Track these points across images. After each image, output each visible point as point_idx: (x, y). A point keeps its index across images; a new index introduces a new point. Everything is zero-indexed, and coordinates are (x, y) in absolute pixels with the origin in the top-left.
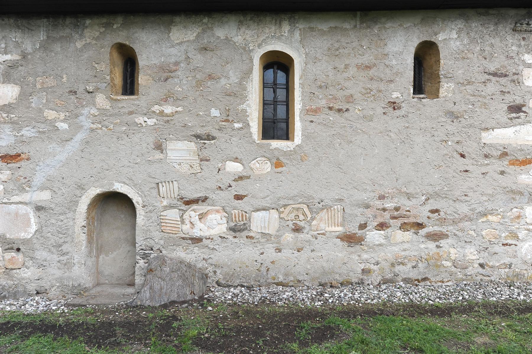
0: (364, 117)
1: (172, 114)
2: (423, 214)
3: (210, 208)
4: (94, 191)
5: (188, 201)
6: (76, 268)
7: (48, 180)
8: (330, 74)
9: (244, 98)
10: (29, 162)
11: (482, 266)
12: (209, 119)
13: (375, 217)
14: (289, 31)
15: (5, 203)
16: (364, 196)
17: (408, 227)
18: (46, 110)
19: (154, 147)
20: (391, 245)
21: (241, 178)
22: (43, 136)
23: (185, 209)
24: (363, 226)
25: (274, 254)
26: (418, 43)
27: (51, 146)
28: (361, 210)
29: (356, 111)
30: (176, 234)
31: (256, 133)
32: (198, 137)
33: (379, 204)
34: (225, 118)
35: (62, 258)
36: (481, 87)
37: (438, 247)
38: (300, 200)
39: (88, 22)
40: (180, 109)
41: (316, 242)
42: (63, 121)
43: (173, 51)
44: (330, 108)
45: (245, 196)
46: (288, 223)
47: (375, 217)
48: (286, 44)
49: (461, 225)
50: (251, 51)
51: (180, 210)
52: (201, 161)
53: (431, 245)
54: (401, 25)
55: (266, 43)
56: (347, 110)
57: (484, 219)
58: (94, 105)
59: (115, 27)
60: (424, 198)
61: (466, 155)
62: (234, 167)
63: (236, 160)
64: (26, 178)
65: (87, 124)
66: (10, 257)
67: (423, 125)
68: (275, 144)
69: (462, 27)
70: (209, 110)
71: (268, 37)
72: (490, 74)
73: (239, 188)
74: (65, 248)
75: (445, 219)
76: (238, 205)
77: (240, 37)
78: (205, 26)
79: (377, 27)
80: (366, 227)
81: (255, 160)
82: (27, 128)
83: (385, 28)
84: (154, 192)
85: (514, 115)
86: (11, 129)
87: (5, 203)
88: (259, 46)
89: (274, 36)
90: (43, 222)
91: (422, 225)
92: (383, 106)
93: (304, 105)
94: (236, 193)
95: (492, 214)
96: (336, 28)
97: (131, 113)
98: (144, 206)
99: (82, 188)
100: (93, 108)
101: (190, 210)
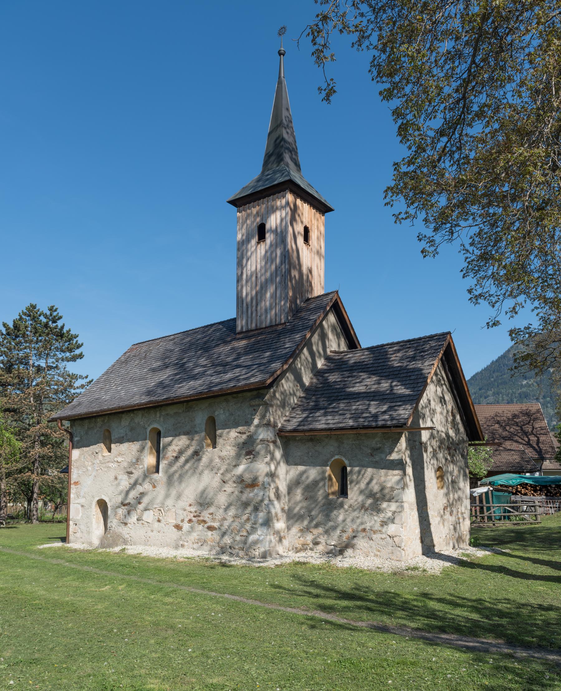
13: (187, 515)
24: (182, 521)
28: (182, 511)
43: (122, 431)
54: (200, 408)
85: (248, 457)
88: (149, 426)
97: (108, 462)
99: (93, 497)
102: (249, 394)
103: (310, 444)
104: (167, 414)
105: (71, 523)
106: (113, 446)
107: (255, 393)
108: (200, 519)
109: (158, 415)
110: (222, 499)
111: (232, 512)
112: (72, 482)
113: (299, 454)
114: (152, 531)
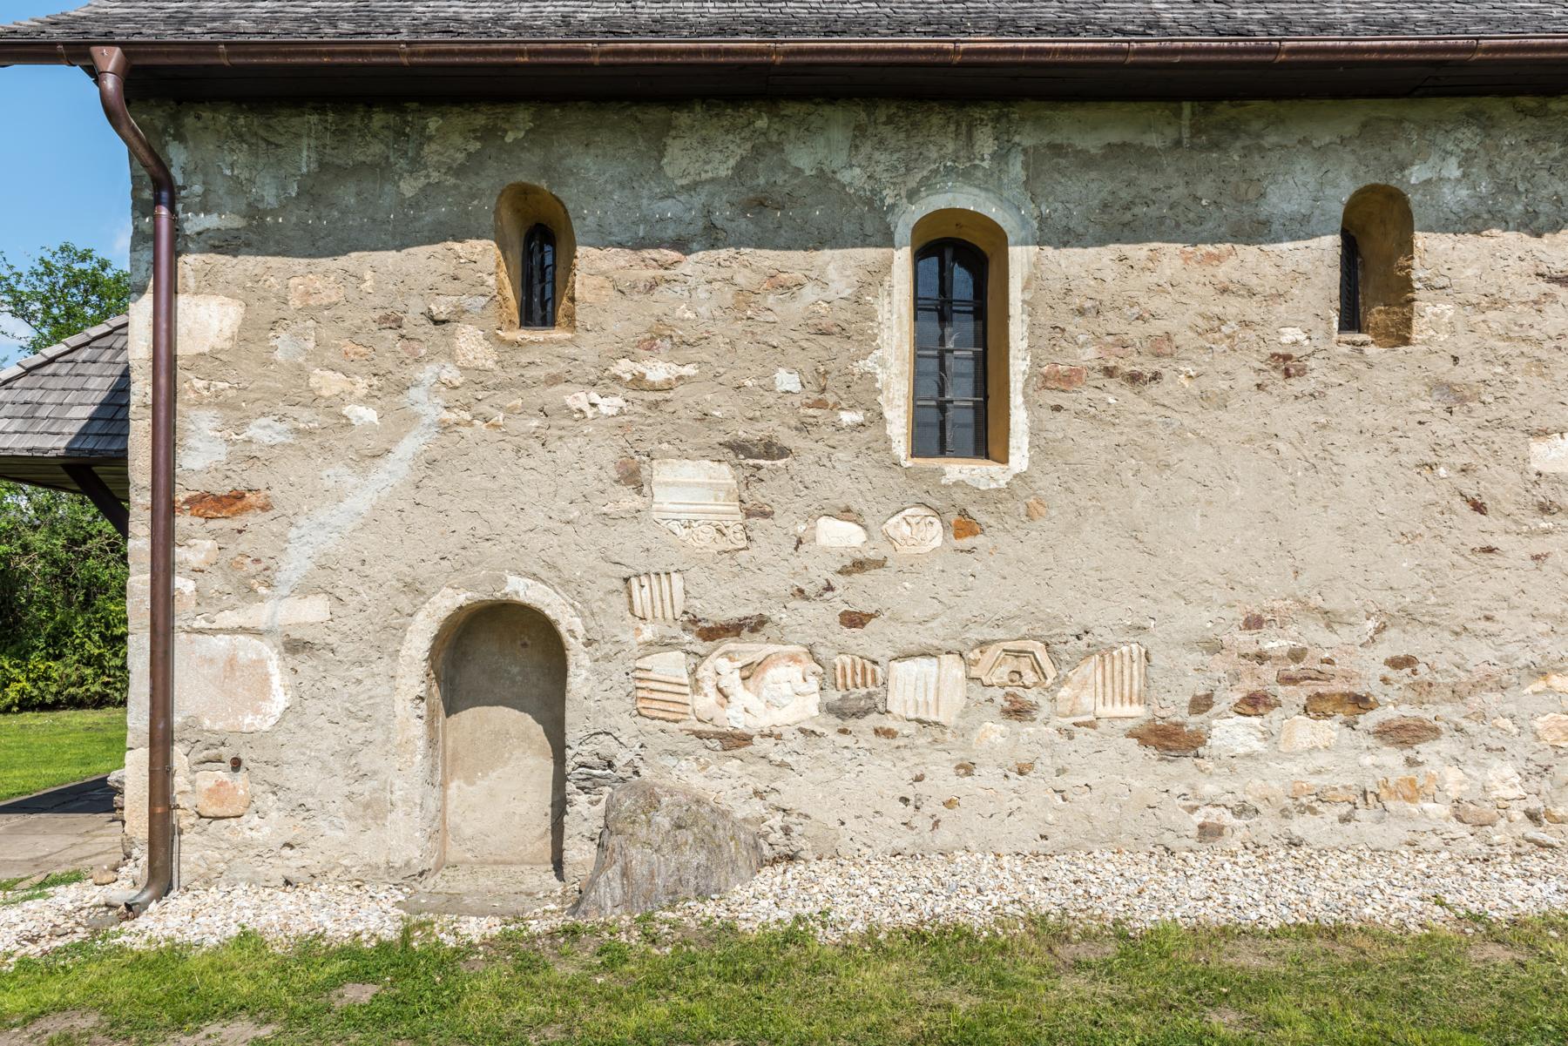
0: (1204, 397)
1: (668, 387)
2: (1367, 669)
3: (772, 648)
4: (448, 601)
5: (710, 630)
6: (397, 815)
7: (322, 567)
8: (1109, 275)
9: (868, 343)
10: (270, 515)
11: (1532, 816)
12: (770, 399)
14: (993, 156)
15: (200, 631)
16: (1201, 620)
17: (1328, 707)
18: (317, 371)
19: (617, 477)
20: (1281, 757)
21: (860, 566)
22: (306, 443)
23: (702, 651)
24: (1201, 704)
25: (954, 780)
26: (1352, 190)
27: (330, 471)
28: (1196, 657)
29: (1177, 382)
30: (677, 721)
31: (902, 439)
32: (739, 448)
33: (1246, 640)
34: (816, 396)
35: (356, 788)
36: (1529, 316)
37: (1411, 763)
38: (1024, 630)
39: (433, 123)
40: (689, 370)
41: (1071, 746)
42: (367, 400)
44: (1109, 372)
45: (871, 616)
46: (990, 692)
47: (1237, 677)
48: (987, 190)
49: (1475, 702)
51: (688, 653)
52: (749, 514)
53: (1392, 758)
54: (1304, 141)
55: (929, 187)
56: (1156, 377)
57: (1540, 685)
58: (451, 356)
59: (509, 138)
60: (1371, 625)
61: (1489, 504)
62: (839, 536)
63: (846, 513)
64: (257, 561)
65: (432, 411)
66: (211, 784)
67: (1367, 422)
68: (959, 470)
69: (1474, 146)
70: (770, 375)
71: (937, 171)
72: (1552, 280)
73: (854, 593)
74: (366, 760)
75: (1430, 685)
76: (851, 642)
77: (857, 171)
78: (762, 139)
79: (1238, 144)
80: (1209, 706)
81: (899, 517)
82: (263, 421)
83: (1260, 148)
84: (619, 602)
86: (217, 424)
87: (200, 631)
88: (912, 195)
89: (953, 169)
90: (306, 685)
91: (1365, 700)
92: (1258, 365)
93: (1036, 363)
94: (846, 607)
95: (1560, 670)
96: (1124, 145)
97: (554, 380)
98: (589, 643)
99: (415, 589)
100: (450, 367)
101: (716, 653)
108: (1322, 688)
109: (986, 143)
114: (967, 769)
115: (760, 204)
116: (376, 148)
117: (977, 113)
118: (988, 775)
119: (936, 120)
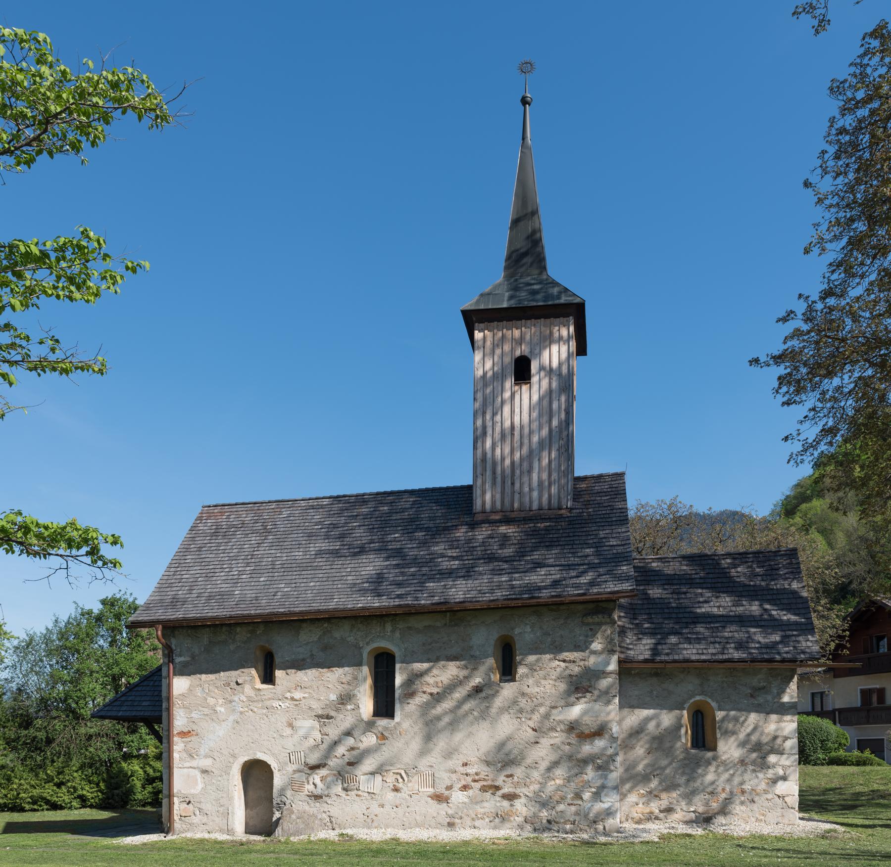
22: (207, 718)
24: (449, 788)
28: (448, 774)
33: (463, 770)
50: (361, 648)
53: (506, 803)
54: (483, 622)
88: (368, 644)
96: (429, 626)
99: (234, 756)
102: (580, 607)
103: (654, 680)
104: (410, 628)
105: (176, 800)
106: (279, 673)
107: (591, 606)
110: (543, 753)
111: (560, 773)
112: (175, 732)
113: (636, 693)
114: (382, 806)
115: (325, 648)
116: (224, 637)
117: (386, 619)
118: (388, 807)
119: (374, 622)
